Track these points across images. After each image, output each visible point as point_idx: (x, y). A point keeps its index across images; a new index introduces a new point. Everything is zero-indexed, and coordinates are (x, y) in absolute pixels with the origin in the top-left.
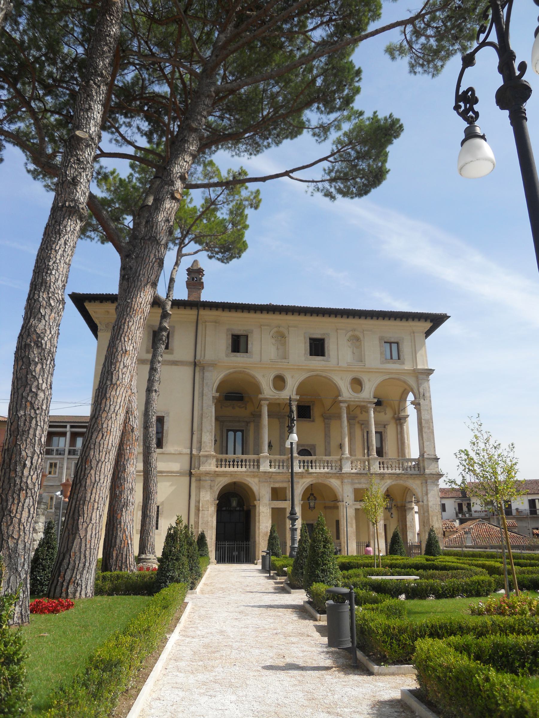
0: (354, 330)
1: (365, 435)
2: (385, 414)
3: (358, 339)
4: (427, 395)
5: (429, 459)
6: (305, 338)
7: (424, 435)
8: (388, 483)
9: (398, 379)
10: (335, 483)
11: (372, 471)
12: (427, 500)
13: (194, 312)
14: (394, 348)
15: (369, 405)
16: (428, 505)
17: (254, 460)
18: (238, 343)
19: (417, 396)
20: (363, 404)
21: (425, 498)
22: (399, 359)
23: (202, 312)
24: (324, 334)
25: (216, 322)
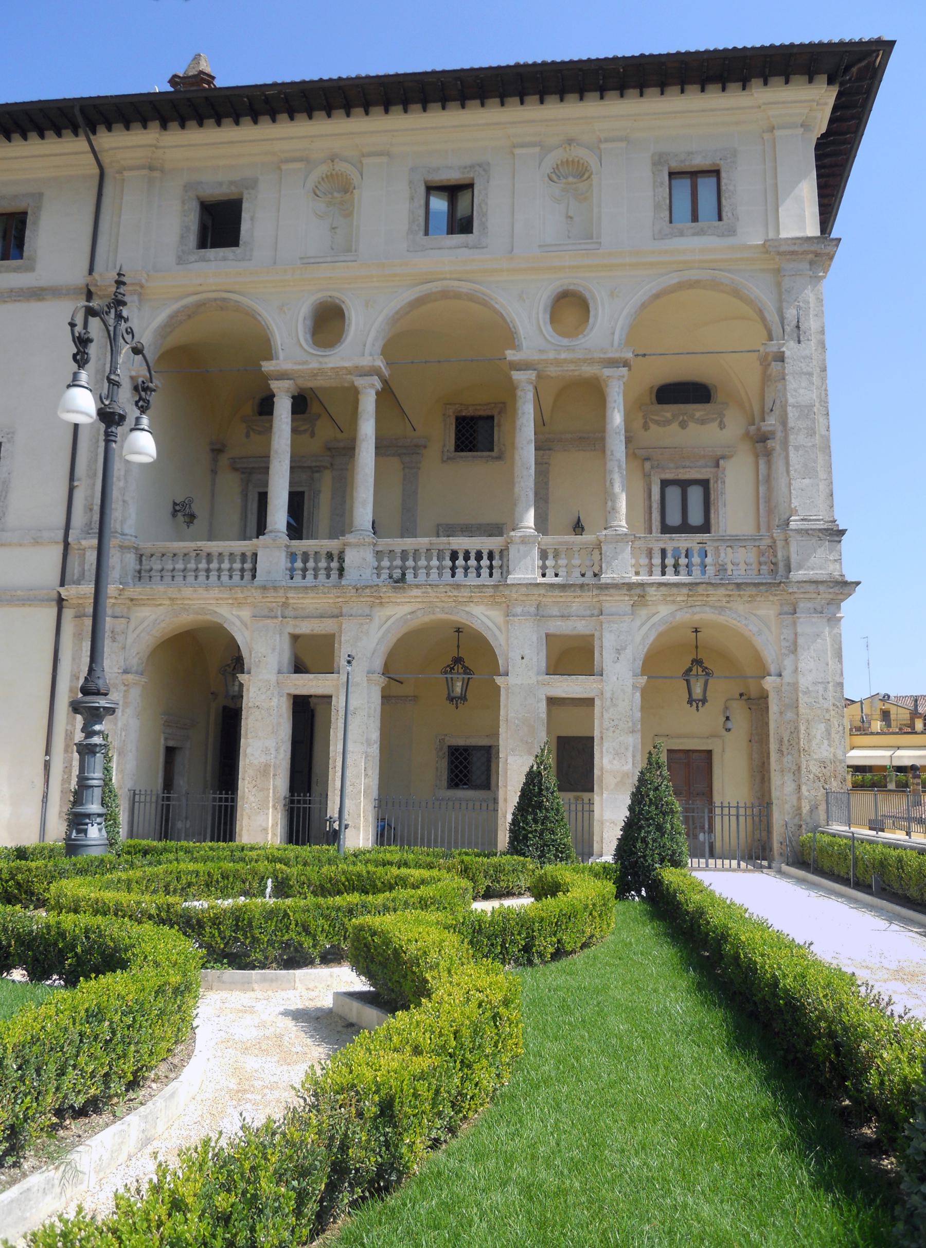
0: (570, 141)
2: (722, 426)
4: (811, 324)
5: (806, 532)
6: (411, 182)
7: (792, 454)
9: (714, 285)
10: (483, 616)
11: (606, 578)
12: (796, 670)
13: (79, 144)
14: (696, 185)
15: (607, 372)
16: (795, 686)
17: (243, 555)
18: (219, 224)
19: (776, 329)
20: (588, 370)
21: (788, 663)
22: (720, 218)
23: (106, 140)
24: (472, 167)
25: (151, 168)
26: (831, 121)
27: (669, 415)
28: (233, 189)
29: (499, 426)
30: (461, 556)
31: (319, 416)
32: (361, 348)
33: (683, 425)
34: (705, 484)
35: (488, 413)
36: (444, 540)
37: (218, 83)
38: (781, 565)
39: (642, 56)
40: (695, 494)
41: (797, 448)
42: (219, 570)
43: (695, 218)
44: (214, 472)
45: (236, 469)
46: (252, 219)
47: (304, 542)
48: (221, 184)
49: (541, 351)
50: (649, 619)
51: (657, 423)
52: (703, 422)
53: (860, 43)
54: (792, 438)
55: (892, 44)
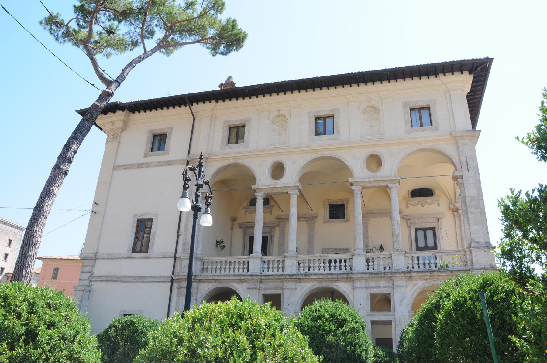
1: (413, 232)
3: (376, 110)
7: (470, 215)
8: (420, 284)
19: (459, 167)
20: (382, 184)
22: (431, 125)
26: (472, 87)
27: (416, 202)
28: (242, 122)
29: (347, 208)
30: (333, 262)
31: (274, 206)
32: (291, 178)
33: (422, 205)
34: (433, 229)
35: (342, 203)
36: (326, 255)
37: (237, 85)
38: (469, 262)
39: (396, 68)
40: (430, 233)
41: (471, 213)
42: (234, 268)
43: (421, 125)
44: (232, 229)
45: (241, 228)
46: (249, 133)
47: (268, 257)
48: (237, 121)
49: (363, 178)
50: (414, 287)
51: (412, 205)
52: (431, 204)
53: (480, 59)
54: (469, 209)
55: (493, 59)
